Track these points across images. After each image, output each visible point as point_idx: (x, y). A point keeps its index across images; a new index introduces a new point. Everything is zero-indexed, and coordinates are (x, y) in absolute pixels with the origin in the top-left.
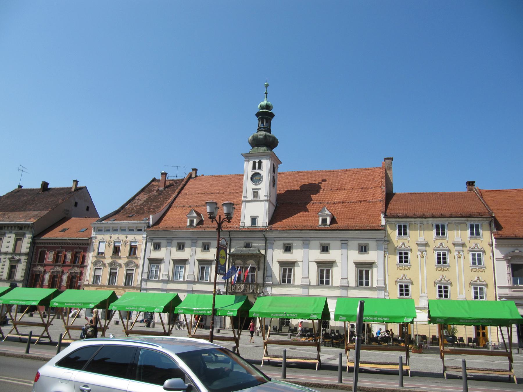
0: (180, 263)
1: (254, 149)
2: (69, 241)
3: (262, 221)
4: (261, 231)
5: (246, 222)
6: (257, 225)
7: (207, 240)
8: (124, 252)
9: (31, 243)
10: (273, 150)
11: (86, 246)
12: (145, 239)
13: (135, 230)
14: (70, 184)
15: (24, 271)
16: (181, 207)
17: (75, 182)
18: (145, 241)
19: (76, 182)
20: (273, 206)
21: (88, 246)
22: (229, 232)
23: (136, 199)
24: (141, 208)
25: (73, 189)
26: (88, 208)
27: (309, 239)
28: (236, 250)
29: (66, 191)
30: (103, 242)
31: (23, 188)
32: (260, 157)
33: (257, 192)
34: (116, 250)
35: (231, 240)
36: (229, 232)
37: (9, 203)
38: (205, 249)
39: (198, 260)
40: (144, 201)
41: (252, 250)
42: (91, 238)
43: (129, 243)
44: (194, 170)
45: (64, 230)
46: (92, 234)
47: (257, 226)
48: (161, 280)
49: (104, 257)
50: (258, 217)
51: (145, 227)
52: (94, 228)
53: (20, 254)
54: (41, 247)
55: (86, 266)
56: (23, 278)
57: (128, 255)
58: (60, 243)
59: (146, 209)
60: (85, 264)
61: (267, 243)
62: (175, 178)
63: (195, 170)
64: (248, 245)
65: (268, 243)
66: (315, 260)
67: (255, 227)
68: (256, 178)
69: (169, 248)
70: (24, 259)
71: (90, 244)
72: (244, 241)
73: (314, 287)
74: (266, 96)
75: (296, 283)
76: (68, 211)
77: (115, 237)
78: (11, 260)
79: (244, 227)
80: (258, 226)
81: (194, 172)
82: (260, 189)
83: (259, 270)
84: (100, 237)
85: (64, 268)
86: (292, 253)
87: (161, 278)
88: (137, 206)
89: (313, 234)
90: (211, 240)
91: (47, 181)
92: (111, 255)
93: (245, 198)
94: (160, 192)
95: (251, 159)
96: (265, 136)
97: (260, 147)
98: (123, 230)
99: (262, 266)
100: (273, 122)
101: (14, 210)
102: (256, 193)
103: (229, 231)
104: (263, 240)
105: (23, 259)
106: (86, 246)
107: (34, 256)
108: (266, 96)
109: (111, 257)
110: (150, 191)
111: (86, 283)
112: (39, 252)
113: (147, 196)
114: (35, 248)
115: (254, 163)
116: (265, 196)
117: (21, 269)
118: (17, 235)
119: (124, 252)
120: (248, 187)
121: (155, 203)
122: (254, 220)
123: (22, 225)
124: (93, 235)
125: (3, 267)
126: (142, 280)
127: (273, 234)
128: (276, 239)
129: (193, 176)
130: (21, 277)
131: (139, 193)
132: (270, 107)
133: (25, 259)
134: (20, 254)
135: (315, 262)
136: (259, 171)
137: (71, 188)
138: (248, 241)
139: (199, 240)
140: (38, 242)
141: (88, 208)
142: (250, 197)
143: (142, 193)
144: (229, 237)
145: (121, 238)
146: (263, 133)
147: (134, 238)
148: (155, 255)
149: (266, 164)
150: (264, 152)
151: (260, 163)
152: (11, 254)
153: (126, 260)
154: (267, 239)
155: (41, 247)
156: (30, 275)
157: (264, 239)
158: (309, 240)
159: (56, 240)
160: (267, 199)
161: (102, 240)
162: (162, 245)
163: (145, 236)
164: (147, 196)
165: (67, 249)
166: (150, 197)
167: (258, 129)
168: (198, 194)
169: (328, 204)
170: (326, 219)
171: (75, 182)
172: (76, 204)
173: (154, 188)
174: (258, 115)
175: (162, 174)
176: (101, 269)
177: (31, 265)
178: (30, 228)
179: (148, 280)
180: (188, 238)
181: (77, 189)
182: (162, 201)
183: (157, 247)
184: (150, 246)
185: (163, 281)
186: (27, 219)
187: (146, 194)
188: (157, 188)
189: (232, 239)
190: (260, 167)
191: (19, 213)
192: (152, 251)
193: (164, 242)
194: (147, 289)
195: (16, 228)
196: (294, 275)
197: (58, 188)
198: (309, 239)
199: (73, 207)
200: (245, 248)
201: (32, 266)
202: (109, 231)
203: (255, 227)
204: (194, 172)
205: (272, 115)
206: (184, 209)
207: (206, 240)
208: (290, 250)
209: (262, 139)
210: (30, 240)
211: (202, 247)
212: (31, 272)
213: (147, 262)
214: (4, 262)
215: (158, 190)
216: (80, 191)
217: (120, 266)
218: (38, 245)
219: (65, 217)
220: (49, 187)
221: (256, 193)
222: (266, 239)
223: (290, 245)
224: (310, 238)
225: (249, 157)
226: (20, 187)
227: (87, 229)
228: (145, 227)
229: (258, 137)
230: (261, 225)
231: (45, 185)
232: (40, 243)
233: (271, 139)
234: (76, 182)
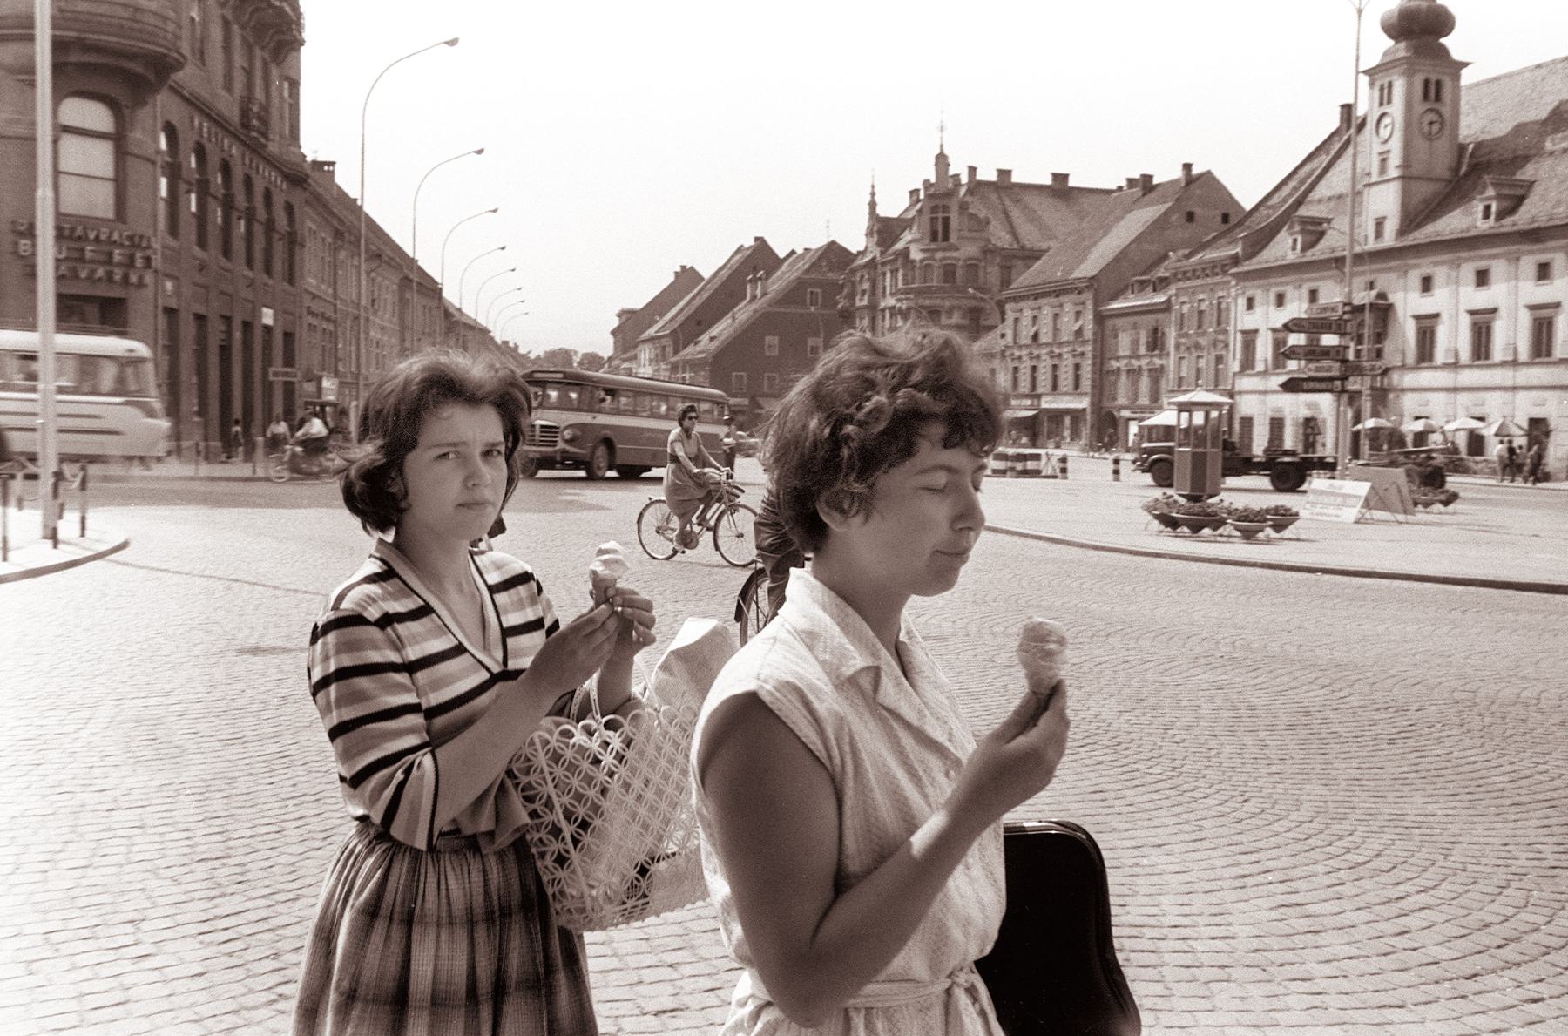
19: (1187, 167)
82: (1388, 151)
122: (1380, 224)
220: (1156, 181)
234: (1187, 167)
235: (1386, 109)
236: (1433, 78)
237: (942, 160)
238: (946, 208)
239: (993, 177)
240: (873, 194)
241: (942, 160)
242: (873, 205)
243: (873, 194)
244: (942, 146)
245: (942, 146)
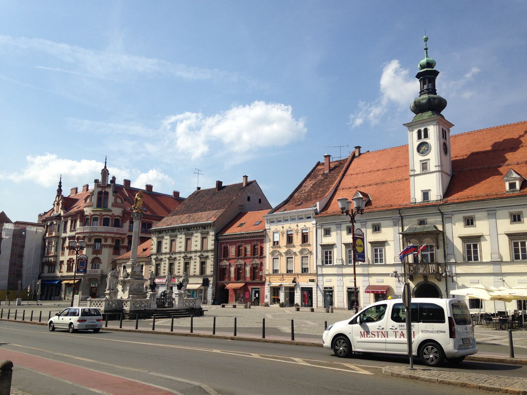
1: (418, 117)
2: (247, 235)
3: (435, 195)
4: (436, 206)
5: (419, 198)
6: (430, 200)
7: (378, 221)
8: (297, 240)
9: (214, 240)
10: (441, 113)
11: (262, 238)
12: (315, 226)
13: (304, 218)
14: (240, 180)
15: (213, 266)
16: (347, 189)
17: (245, 178)
18: (315, 228)
19: (246, 177)
20: (447, 176)
21: (264, 238)
22: (399, 210)
23: (303, 186)
24: (308, 195)
25: (244, 185)
26: (260, 201)
27: (495, 209)
28: (409, 229)
29: (239, 187)
30: (277, 232)
31: (201, 189)
32: (425, 124)
33: (426, 163)
34: (290, 239)
35: (402, 219)
36: (399, 210)
37: (192, 205)
38: (376, 230)
39: (370, 242)
40: (311, 187)
41: (428, 228)
42: (265, 230)
43: (300, 231)
44: (356, 148)
45: (241, 225)
46: (266, 226)
47: (430, 201)
48: (336, 265)
49: (280, 247)
50: (430, 190)
51: (313, 214)
52: (267, 220)
53: (207, 251)
54: (224, 243)
55: (265, 257)
56: (213, 273)
57: (301, 244)
58: (239, 238)
59: (313, 195)
60: (264, 255)
61: (444, 218)
62: (339, 159)
63: (358, 148)
64: (422, 223)
65: (445, 218)
66: (505, 232)
67: (428, 201)
68: (423, 148)
69: (339, 232)
70: (211, 255)
71: (266, 235)
72: (418, 218)
73: (507, 263)
74: (427, 52)
75: (484, 260)
76: (242, 206)
77: (287, 226)
78: (201, 257)
79: (415, 203)
80: (431, 200)
81: (358, 150)
82: (429, 160)
83: (438, 248)
84: (273, 228)
85: (246, 261)
86: (476, 227)
87: (335, 263)
88: (304, 193)
89: (498, 203)
90: (381, 220)
91: (220, 180)
92: (285, 245)
93: (413, 172)
94: (325, 176)
95: (416, 128)
96: (429, 99)
97: (424, 113)
98: (293, 219)
99: (441, 244)
100: (438, 80)
101: (196, 211)
102: (424, 165)
103: (399, 210)
104: (438, 215)
105: (210, 254)
106: (262, 238)
107: (219, 252)
108: (427, 52)
109: (286, 246)
110: (316, 177)
111: (267, 273)
112: (223, 247)
113: (313, 182)
114: (219, 244)
115: (419, 132)
116: (436, 166)
117: (210, 265)
118: (202, 234)
119: (297, 240)
120: (416, 159)
121: (322, 188)
122: (426, 194)
123: (205, 224)
124: (267, 226)
125: (195, 264)
126: (317, 266)
127: (450, 208)
128: (454, 212)
129: (357, 154)
130: (211, 272)
131: (305, 180)
132: (432, 64)
133: (212, 255)
134: (207, 251)
135: (505, 235)
136: (426, 140)
137: (242, 184)
138: (422, 218)
139: (368, 222)
140: (220, 239)
141: (260, 201)
142: (418, 170)
143: (308, 180)
144: (400, 215)
145: (292, 228)
146: (426, 96)
147: (305, 226)
148: (327, 241)
149: (433, 130)
150: (429, 117)
151: (426, 131)
152: (200, 251)
153: (300, 248)
154: (444, 213)
155: (224, 243)
156: (218, 269)
157: (440, 214)
158: (496, 210)
159: (235, 235)
160: (438, 170)
161: (276, 231)
162: (332, 230)
163: (314, 222)
164: (313, 182)
165: (246, 242)
166: (316, 183)
167: (420, 93)
168: (364, 173)
169: (518, 164)
170: (515, 183)
171: (245, 178)
172: (249, 199)
173: (319, 173)
174: (418, 76)
175: (325, 156)
176: (278, 258)
177: (217, 260)
178: (212, 227)
179: (322, 266)
181: (248, 184)
182: (328, 185)
183: (327, 232)
184: (321, 232)
185: (337, 266)
186: (208, 219)
187: (312, 180)
188: (322, 172)
189: (403, 217)
190: (426, 136)
191: (201, 213)
192: (323, 237)
193: (333, 227)
194: (323, 275)
196: (481, 251)
197: (231, 186)
198: (495, 209)
199: (247, 202)
200: (419, 226)
201: (219, 261)
202: (280, 221)
203: (428, 201)
204: (358, 150)
205: (436, 73)
206: (350, 191)
207: (375, 221)
208: (472, 224)
209: (425, 103)
210: (213, 238)
211: (373, 228)
212: (218, 267)
213: (319, 248)
214: (195, 259)
215: (324, 174)
216: (251, 186)
217: (295, 254)
218: (221, 241)
219: (241, 212)
220: (223, 185)
221: (424, 165)
222: (442, 214)
223: (472, 218)
224: (496, 207)
225: (413, 127)
226: (199, 188)
227: (261, 221)
228: (313, 214)
229: (421, 101)
230: (435, 199)
231: (219, 183)
232: (222, 239)
233: (436, 101)
234: (246, 177)
235: (423, 140)
236: (444, 129)
237: (105, 173)
238: (107, 193)
239: (122, 183)
240: (60, 186)
241: (105, 173)
242: (60, 191)
243: (60, 186)
244: (105, 167)
245: (105, 167)
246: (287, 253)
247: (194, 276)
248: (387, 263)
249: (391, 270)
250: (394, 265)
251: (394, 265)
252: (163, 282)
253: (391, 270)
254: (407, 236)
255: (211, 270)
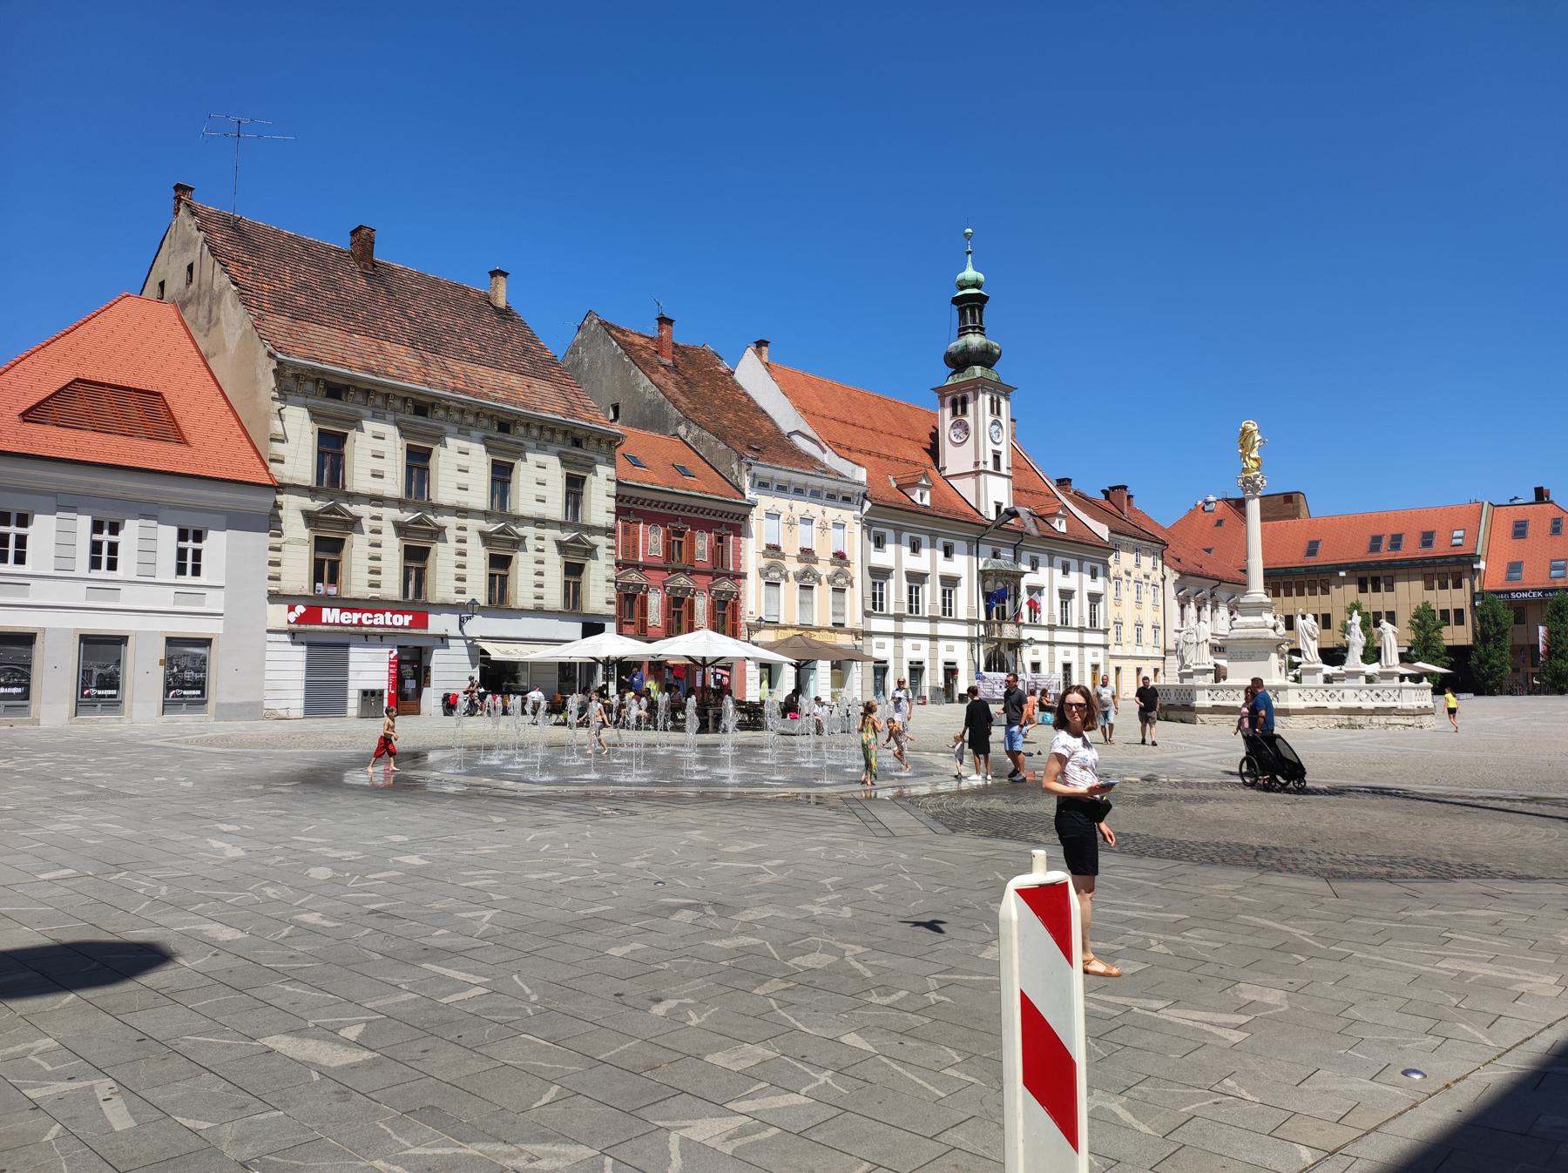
0: (916, 579)
11: (737, 522)
21: (742, 523)
84: (766, 502)
106: (737, 522)
109: (798, 557)
124: (750, 495)
180: (924, 532)
183: (879, 542)
195: (560, 437)
214: (374, 531)
246: (801, 576)
247: (539, 612)
248: (959, 618)
249: (963, 631)
250: (970, 622)
251: (970, 622)
252: (372, 625)
253: (963, 631)
254: (984, 575)
255: (607, 595)
